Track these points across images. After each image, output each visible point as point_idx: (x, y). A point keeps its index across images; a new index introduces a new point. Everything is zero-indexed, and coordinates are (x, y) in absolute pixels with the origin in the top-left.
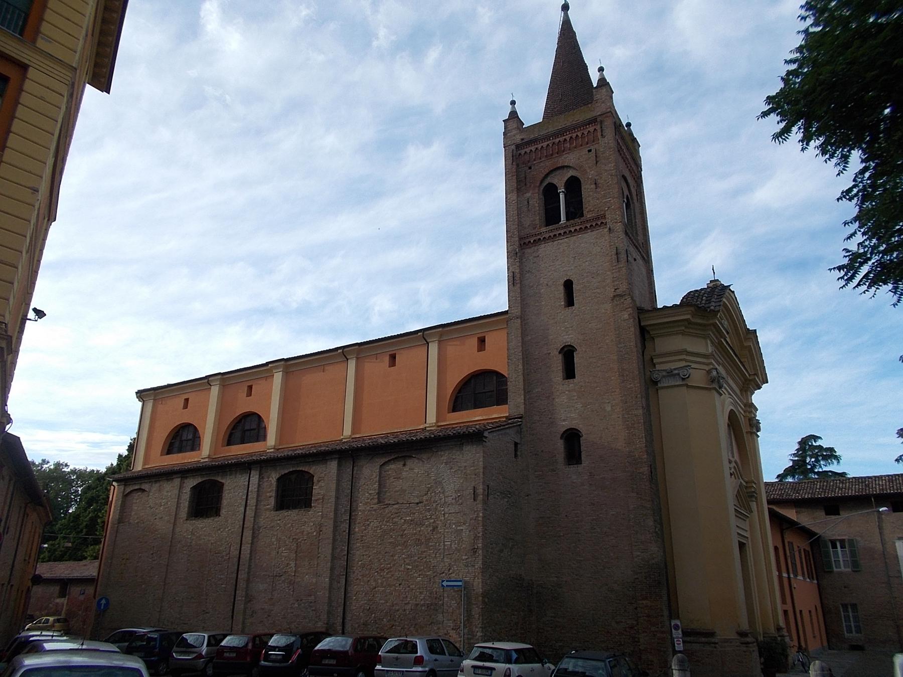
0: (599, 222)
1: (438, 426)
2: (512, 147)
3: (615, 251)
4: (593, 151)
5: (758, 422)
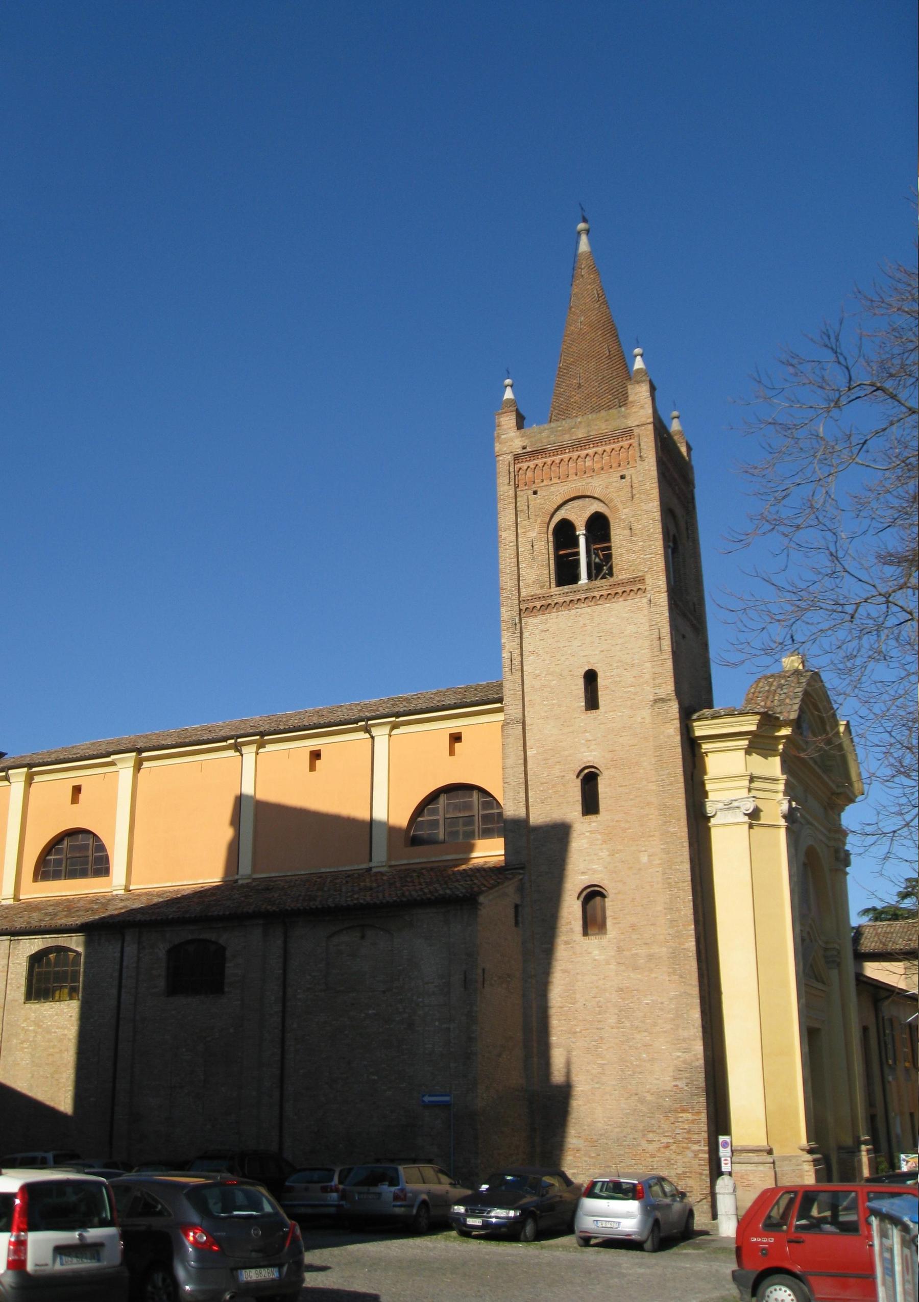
0: (635, 586)
1: (391, 866)
2: (509, 457)
3: (657, 633)
4: (628, 478)
5: (847, 854)
